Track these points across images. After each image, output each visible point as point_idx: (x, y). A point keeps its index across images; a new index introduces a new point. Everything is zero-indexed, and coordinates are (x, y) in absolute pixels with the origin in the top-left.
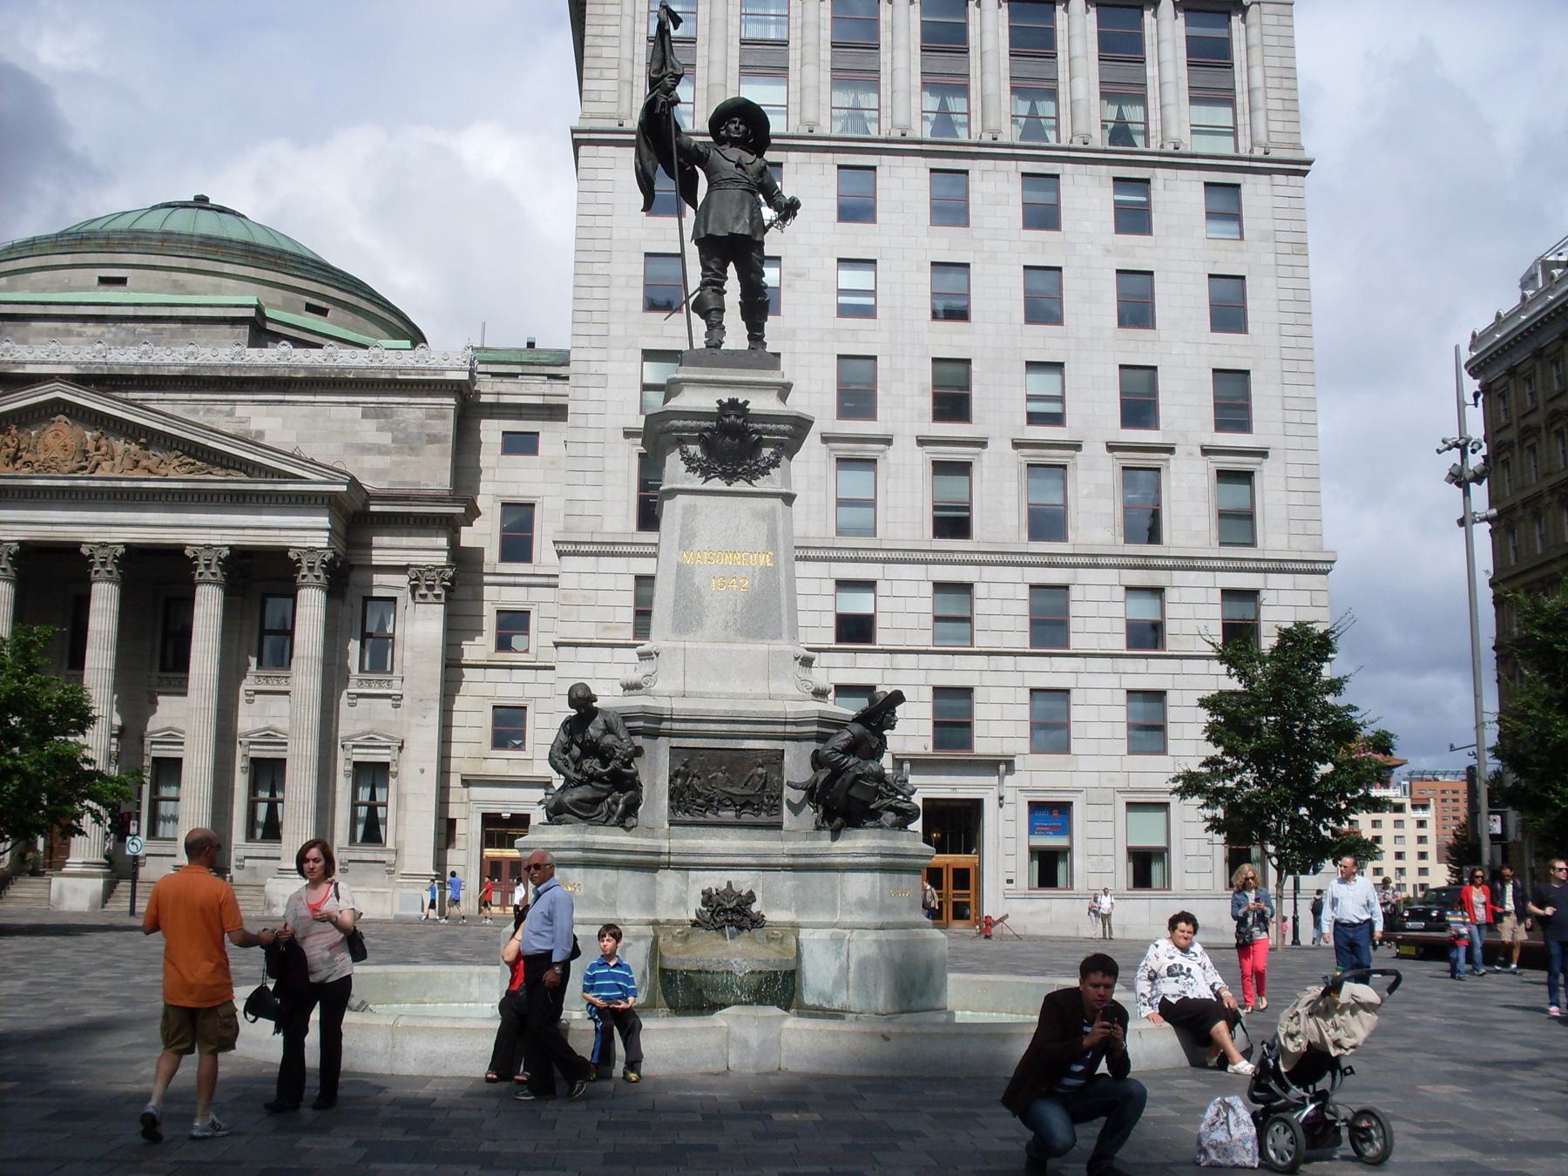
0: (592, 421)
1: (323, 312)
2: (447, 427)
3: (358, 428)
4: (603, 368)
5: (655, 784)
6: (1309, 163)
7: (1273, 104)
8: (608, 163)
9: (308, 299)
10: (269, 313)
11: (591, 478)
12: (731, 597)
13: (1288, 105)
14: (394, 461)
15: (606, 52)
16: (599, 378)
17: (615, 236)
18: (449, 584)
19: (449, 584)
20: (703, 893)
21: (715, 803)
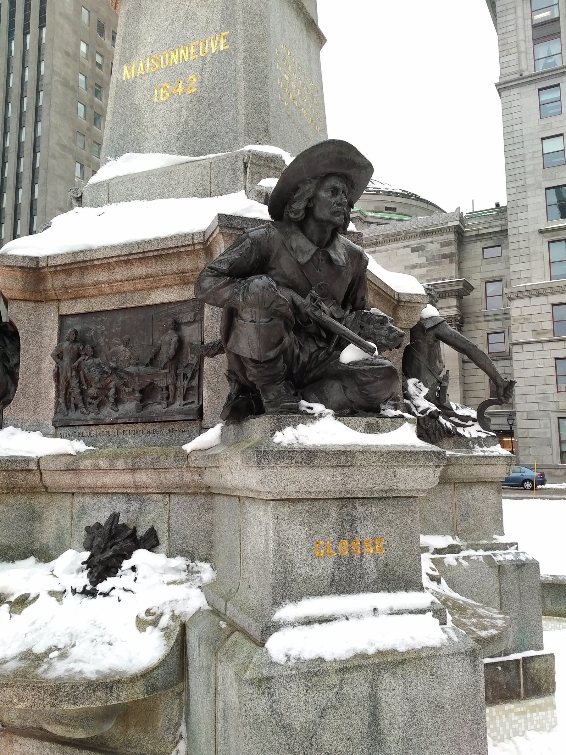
0: (521, 230)
1: (394, 209)
2: (453, 249)
3: (410, 257)
4: (523, 202)
5: (39, 371)
8: (517, 97)
9: (386, 205)
10: (367, 214)
11: (524, 259)
14: (428, 270)
15: (510, 40)
16: (523, 208)
17: (524, 134)
18: (458, 323)
19: (458, 323)
20: (88, 529)
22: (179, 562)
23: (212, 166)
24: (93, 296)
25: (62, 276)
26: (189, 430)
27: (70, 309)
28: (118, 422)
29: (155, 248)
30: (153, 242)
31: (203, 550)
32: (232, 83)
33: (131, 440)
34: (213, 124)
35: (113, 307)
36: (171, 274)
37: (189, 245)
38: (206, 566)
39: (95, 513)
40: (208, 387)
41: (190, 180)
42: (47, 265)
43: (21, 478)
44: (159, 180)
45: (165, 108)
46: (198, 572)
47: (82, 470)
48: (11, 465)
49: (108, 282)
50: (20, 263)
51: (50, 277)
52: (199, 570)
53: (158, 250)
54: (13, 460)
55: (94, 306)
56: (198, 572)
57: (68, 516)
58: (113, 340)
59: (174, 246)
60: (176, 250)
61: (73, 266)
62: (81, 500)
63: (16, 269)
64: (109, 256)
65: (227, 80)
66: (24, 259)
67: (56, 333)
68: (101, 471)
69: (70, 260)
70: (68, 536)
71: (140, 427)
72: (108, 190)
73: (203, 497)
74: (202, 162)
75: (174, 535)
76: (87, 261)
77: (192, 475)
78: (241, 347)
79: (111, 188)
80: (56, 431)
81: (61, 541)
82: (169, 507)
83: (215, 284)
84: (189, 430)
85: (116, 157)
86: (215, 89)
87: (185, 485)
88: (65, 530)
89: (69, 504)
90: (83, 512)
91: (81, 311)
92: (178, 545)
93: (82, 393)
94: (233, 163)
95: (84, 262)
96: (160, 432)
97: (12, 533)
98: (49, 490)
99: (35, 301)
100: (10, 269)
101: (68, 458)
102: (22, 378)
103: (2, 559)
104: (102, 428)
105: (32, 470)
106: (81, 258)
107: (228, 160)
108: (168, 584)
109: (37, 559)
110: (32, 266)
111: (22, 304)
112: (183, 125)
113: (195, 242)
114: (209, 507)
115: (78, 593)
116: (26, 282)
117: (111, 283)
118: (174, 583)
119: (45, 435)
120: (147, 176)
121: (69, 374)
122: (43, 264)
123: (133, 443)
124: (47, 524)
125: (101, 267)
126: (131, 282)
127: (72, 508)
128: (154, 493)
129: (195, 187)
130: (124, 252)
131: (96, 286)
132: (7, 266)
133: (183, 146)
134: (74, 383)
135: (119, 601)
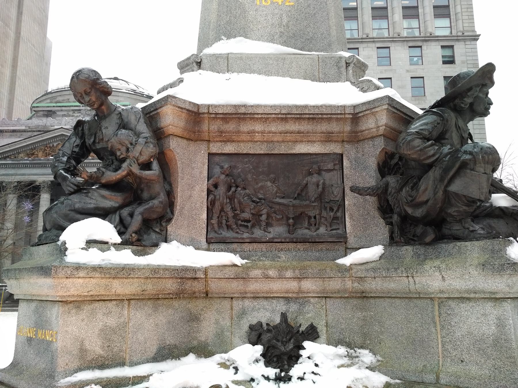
5: (190, 196)
6: (479, 35)
7: (464, 17)
12: (276, 11)
13: (470, 17)
21: (264, 217)
22: (342, 350)
23: (320, 61)
24: (243, 141)
25: (219, 122)
26: (336, 249)
27: (220, 149)
28: (274, 241)
29: (311, 112)
30: (310, 108)
31: (358, 340)
32: (324, 6)
33: (283, 256)
34: (310, 31)
35: (262, 152)
36: (319, 133)
37: (341, 114)
38: (366, 352)
39: (255, 313)
40: (350, 218)
41: (301, 67)
42: (209, 112)
43: (189, 285)
44: (275, 62)
45: (267, 11)
46: (357, 357)
47: (251, 278)
48: (184, 274)
49: (263, 132)
50: (187, 107)
51: (207, 122)
52: (358, 355)
53: (313, 114)
54: (186, 269)
55: (244, 149)
56: (357, 357)
57: (227, 316)
58: (261, 177)
59: (329, 113)
60: (329, 116)
61: (234, 116)
62: (241, 303)
63: (184, 111)
64: (269, 112)
65: (319, 3)
66: (190, 104)
67: (206, 167)
68: (269, 279)
69: (232, 111)
70: (228, 334)
71: (291, 246)
72: (227, 62)
73: (355, 300)
74: (311, 56)
75: (332, 329)
76: (248, 114)
77: (352, 283)
78: (470, 190)
79: (230, 61)
80: (209, 247)
81: (221, 338)
82: (326, 308)
83: (422, 144)
84: (336, 249)
85: (229, 37)
86: (310, 7)
87: (345, 291)
88: (224, 329)
89: (229, 306)
90: (243, 313)
91: (230, 152)
92: (336, 337)
93: (235, 216)
94: (338, 61)
95: (244, 114)
96: (310, 250)
97: (177, 333)
98: (209, 295)
99: (188, 139)
100: (180, 110)
101: (234, 268)
102: (180, 201)
103: (171, 357)
104: (255, 245)
105: (199, 278)
106: (243, 110)
107: (333, 59)
108: (339, 367)
109: (196, 355)
110: (195, 111)
111: (180, 140)
112: (284, 26)
113: (346, 112)
114: (361, 307)
115: (272, 380)
116: (187, 123)
117: (265, 133)
118: (342, 366)
119: (197, 248)
120: (264, 58)
121: (225, 201)
122: (202, 110)
123: (286, 258)
124: (205, 324)
125: (259, 120)
126: (283, 134)
127: (232, 309)
128: (312, 297)
129: (306, 73)
130: (283, 112)
131: (251, 134)
132: (179, 107)
133: (285, 42)
134: (228, 208)
135: (314, 383)
